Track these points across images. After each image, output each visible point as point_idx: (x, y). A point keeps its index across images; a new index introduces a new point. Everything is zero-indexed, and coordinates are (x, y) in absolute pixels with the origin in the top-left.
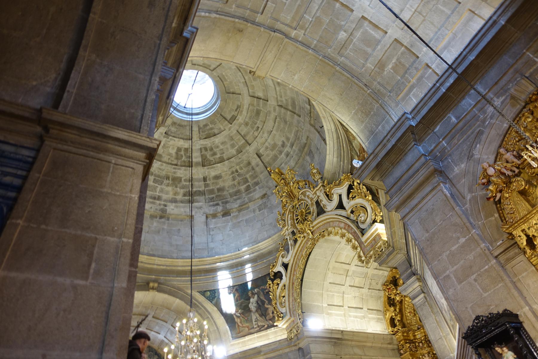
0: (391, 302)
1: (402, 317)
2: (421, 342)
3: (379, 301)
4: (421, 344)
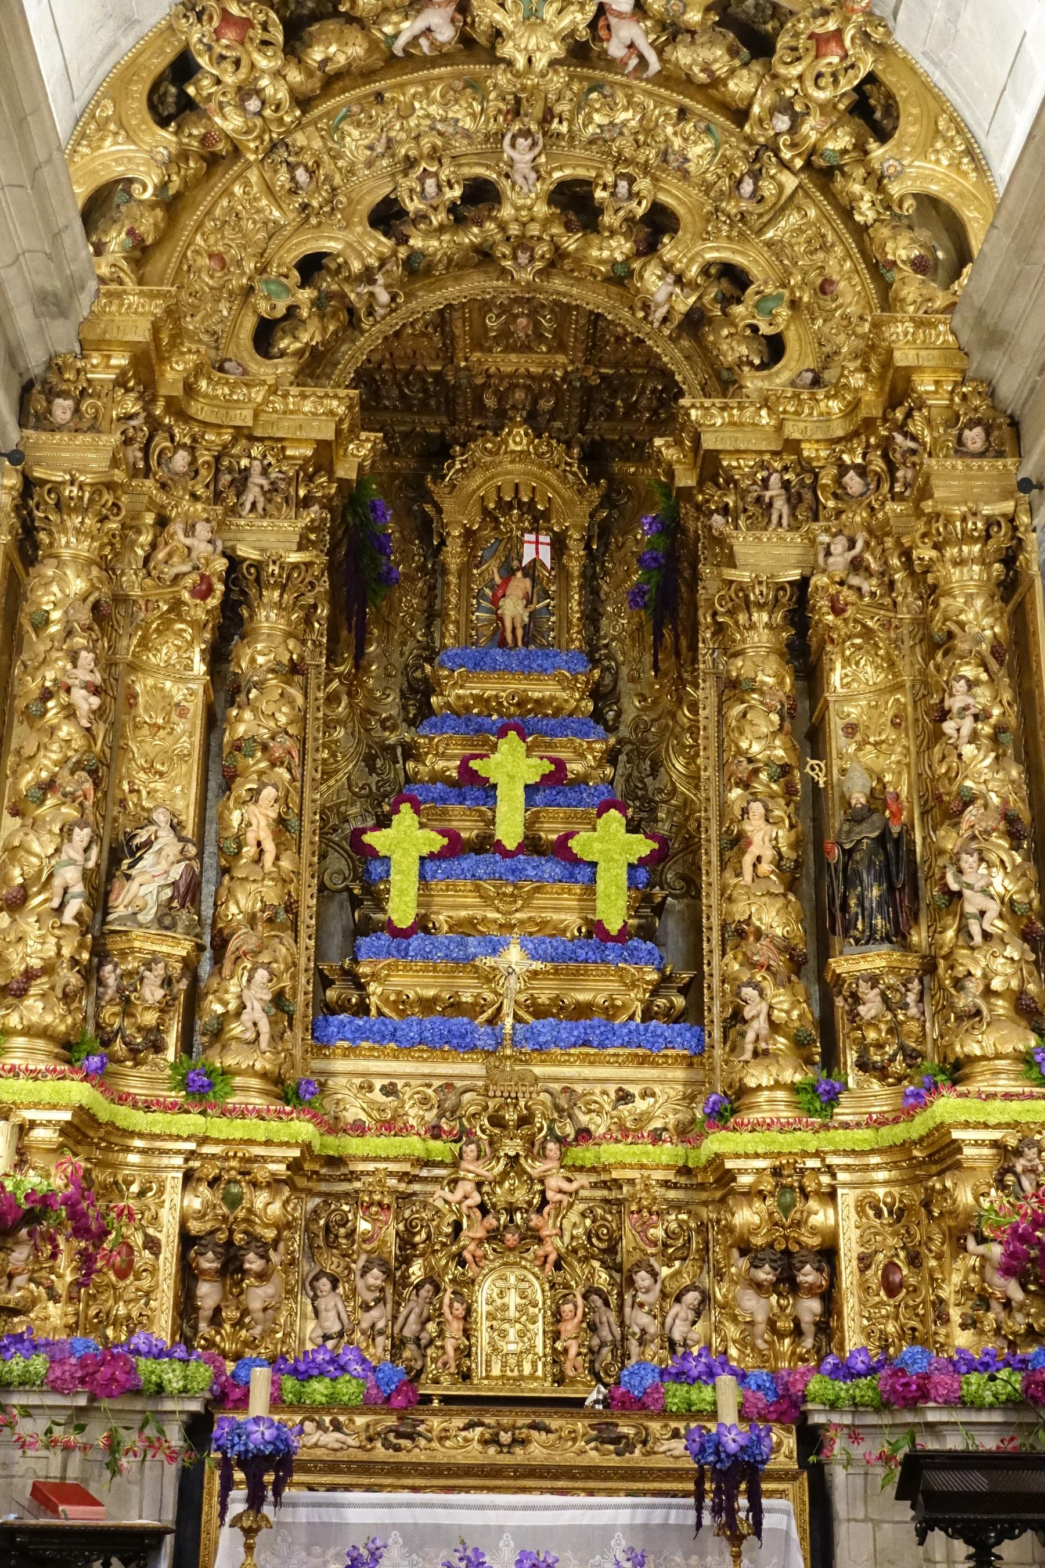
0: (173, 92)
1: (164, 236)
2: (192, 450)
3: (105, 37)
4: (181, 460)
